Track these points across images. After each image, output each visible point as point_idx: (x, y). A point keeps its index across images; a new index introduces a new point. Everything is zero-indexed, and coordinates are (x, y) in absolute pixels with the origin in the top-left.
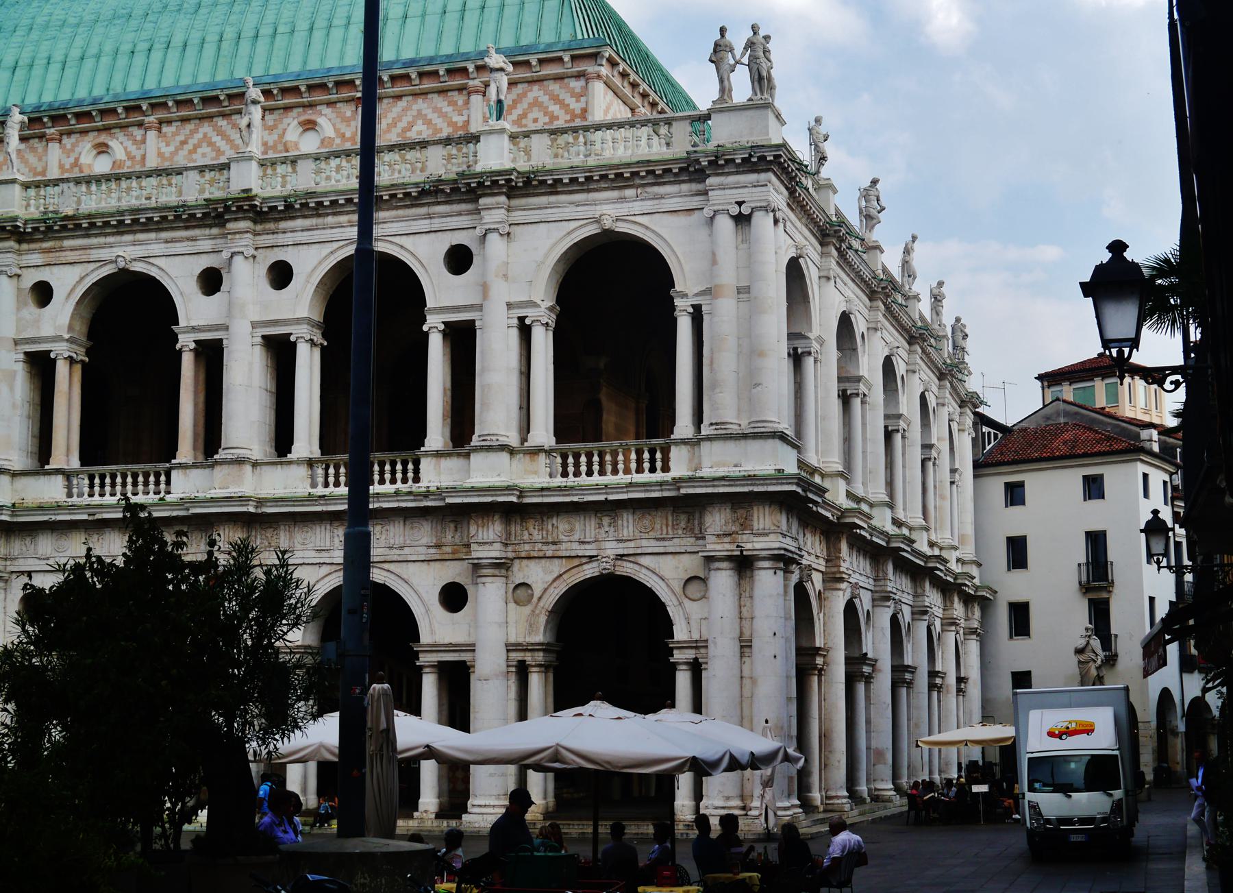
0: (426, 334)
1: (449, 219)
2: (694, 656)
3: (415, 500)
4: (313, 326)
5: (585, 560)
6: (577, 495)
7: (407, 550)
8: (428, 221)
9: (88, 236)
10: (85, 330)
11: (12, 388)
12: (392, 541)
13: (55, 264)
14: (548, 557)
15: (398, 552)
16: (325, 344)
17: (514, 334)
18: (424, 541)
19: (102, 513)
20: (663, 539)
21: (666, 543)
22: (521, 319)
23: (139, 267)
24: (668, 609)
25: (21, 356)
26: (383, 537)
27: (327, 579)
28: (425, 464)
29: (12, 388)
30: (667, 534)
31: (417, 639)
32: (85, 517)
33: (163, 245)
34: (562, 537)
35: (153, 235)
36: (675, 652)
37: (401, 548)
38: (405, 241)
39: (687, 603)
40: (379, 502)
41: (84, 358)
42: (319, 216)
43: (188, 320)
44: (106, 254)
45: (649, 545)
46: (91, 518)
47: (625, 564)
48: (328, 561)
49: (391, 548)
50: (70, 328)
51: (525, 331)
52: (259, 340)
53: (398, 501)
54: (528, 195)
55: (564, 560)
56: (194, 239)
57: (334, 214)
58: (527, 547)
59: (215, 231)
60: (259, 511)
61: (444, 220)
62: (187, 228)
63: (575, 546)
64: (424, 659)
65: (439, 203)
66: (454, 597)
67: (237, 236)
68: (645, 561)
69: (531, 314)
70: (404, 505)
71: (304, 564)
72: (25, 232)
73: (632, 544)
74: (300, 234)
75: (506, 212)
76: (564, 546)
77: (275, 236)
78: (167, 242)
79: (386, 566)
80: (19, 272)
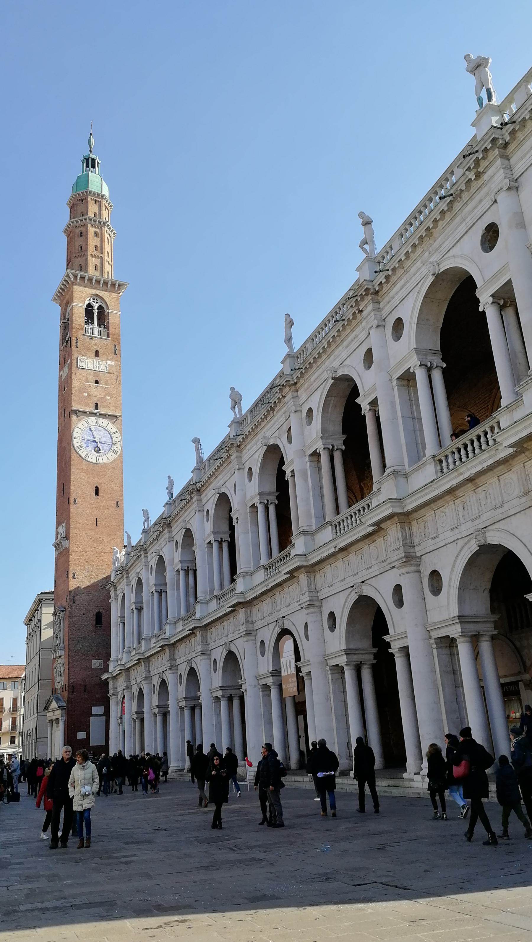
0: (484, 313)
1: (476, 211)
3: (490, 457)
4: (426, 355)
8: (464, 224)
10: (339, 428)
11: (306, 480)
12: (494, 503)
13: (311, 395)
15: (500, 510)
16: (445, 365)
18: (517, 492)
19: (338, 543)
23: (339, 373)
25: (307, 459)
26: (489, 501)
27: (462, 553)
29: (306, 480)
32: (333, 550)
33: (346, 351)
35: (341, 348)
37: (502, 506)
38: (456, 251)
40: (468, 469)
41: (340, 447)
42: (406, 272)
43: (364, 390)
44: (325, 375)
46: (337, 549)
49: (495, 509)
50: (323, 430)
52: (395, 383)
53: (480, 463)
54: (521, 143)
56: (357, 336)
60: (405, 510)
61: (473, 214)
67: (369, 317)
70: (485, 465)
71: (446, 545)
72: (296, 383)
74: (401, 292)
75: (509, 172)
77: (390, 303)
78: (347, 347)
79: (496, 526)
80: (299, 409)
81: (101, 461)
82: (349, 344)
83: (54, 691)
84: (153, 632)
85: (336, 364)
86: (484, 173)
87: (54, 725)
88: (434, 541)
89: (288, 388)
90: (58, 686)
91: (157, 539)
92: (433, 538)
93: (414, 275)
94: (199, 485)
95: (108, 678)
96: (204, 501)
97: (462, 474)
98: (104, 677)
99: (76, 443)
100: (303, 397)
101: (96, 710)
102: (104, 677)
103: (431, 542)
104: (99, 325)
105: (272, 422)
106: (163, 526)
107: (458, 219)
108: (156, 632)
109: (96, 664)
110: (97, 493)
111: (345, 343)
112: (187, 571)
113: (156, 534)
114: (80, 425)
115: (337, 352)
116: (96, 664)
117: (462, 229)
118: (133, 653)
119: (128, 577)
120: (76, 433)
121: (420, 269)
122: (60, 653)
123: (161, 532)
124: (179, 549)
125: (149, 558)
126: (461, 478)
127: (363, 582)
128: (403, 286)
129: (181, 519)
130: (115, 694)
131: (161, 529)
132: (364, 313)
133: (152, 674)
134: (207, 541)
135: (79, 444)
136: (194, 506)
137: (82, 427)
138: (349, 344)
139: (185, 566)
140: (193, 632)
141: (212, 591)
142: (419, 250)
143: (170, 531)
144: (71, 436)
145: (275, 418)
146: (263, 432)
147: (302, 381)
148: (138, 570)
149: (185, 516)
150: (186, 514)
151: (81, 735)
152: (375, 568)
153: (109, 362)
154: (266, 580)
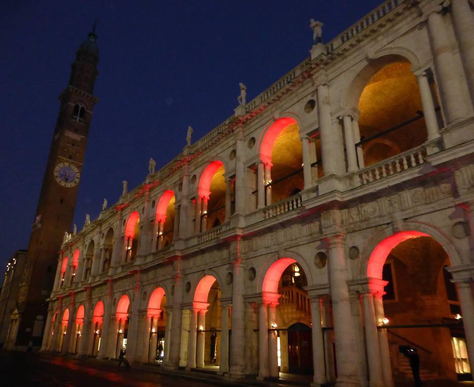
2: (469, 277)
5: (384, 226)
6: (371, 188)
7: (299, 240)
9: (203, 155)
14: (364, 229)
15: (294, 242)
17: (336, 127)
18: (305, 234)
20: (431, 203)
21: (434, 205)
22: (338, 118)
24: (444, 247)
28: (304, 198)
30: (434, 198)
31: (307, 285)
32: (197, 250)
34: (371, 217)
36: (454, 275)
37: (296, 239)
38: (290, 110)
39: (455, 240)
42: (262, 115)
45: (422, 209)
47: (409, 223)
48: (270, 252)
49: (292, 240)
51: (341, 122)
55: (373, 229)
56: (228, 143)
57: (266, 112)
58: (353, 226)
59: (233, 137)
62: (226, 140)
63: (377, 219)
64: (312, 294)
65: (300, 88)
66: (323, 258)
68: (423, 219)
69: (340, 114)
73: (411, 211)
76: (372, 221)
79: (291, 250)
81: (67, 186)
82: (223, 146)
83: (17, 304)
84: (81, 280)
85: (214, 155)
86: (312, 75)
87: (14, 323)
88: (255, 253)
89: (185, 163)
90: (20, 301)
91: (92, 230)
92: (255, 251)
93: (266, 117)
94: (123, 206)
95: (50, 301)
96: (124, 215)
97: (278, 220)
98: (48, 300)
99: (56, 174)
100: (192, 169)
101: (40, 317)
102: (48, 300)
103: (253, 253)
104: (80, 117)
105: (172, 178)
106: (97, 225)
107: (294, 95)
108: (82, 280)
109: (44, 292)
110: (62, 201)
111: (220, 146)
112: (106, 250)
113: (92, 228)
114: (60, 165)
115: (215, 149)
116: (44, 292)
117: (296, 100)
118: (67, 289)
119: (71, 249)
120: (57, 168)
121: (269, 115)
122: (24, 284)
123: (95, 228)
124: (104, 238)
125: (86, 241)
126: (278, 222)
127: (210, 269)
128: (259, 122)
129: (108, 223)
130: (52, 310)
131: (96, 226)
132: (235, 132)
133: (76, 301)
134: (122, 236)
135: (57, 175)
136: (117, 217)
137: (60, 166)
138: (223, 146)
139: (106, 247)
140: (105, 283)
141: (119, 263)
142: (270, 107)
143: (101, 228)
144: (54, 170)
145: (174, 177)
146: (165, 183)
147: (193, 160)
148: (78, 246)
149: (111, 221)
150: (112, 220)
151: (28, 330)
152: (219, 262)
153: (82, 136)
154: (153, 261)
